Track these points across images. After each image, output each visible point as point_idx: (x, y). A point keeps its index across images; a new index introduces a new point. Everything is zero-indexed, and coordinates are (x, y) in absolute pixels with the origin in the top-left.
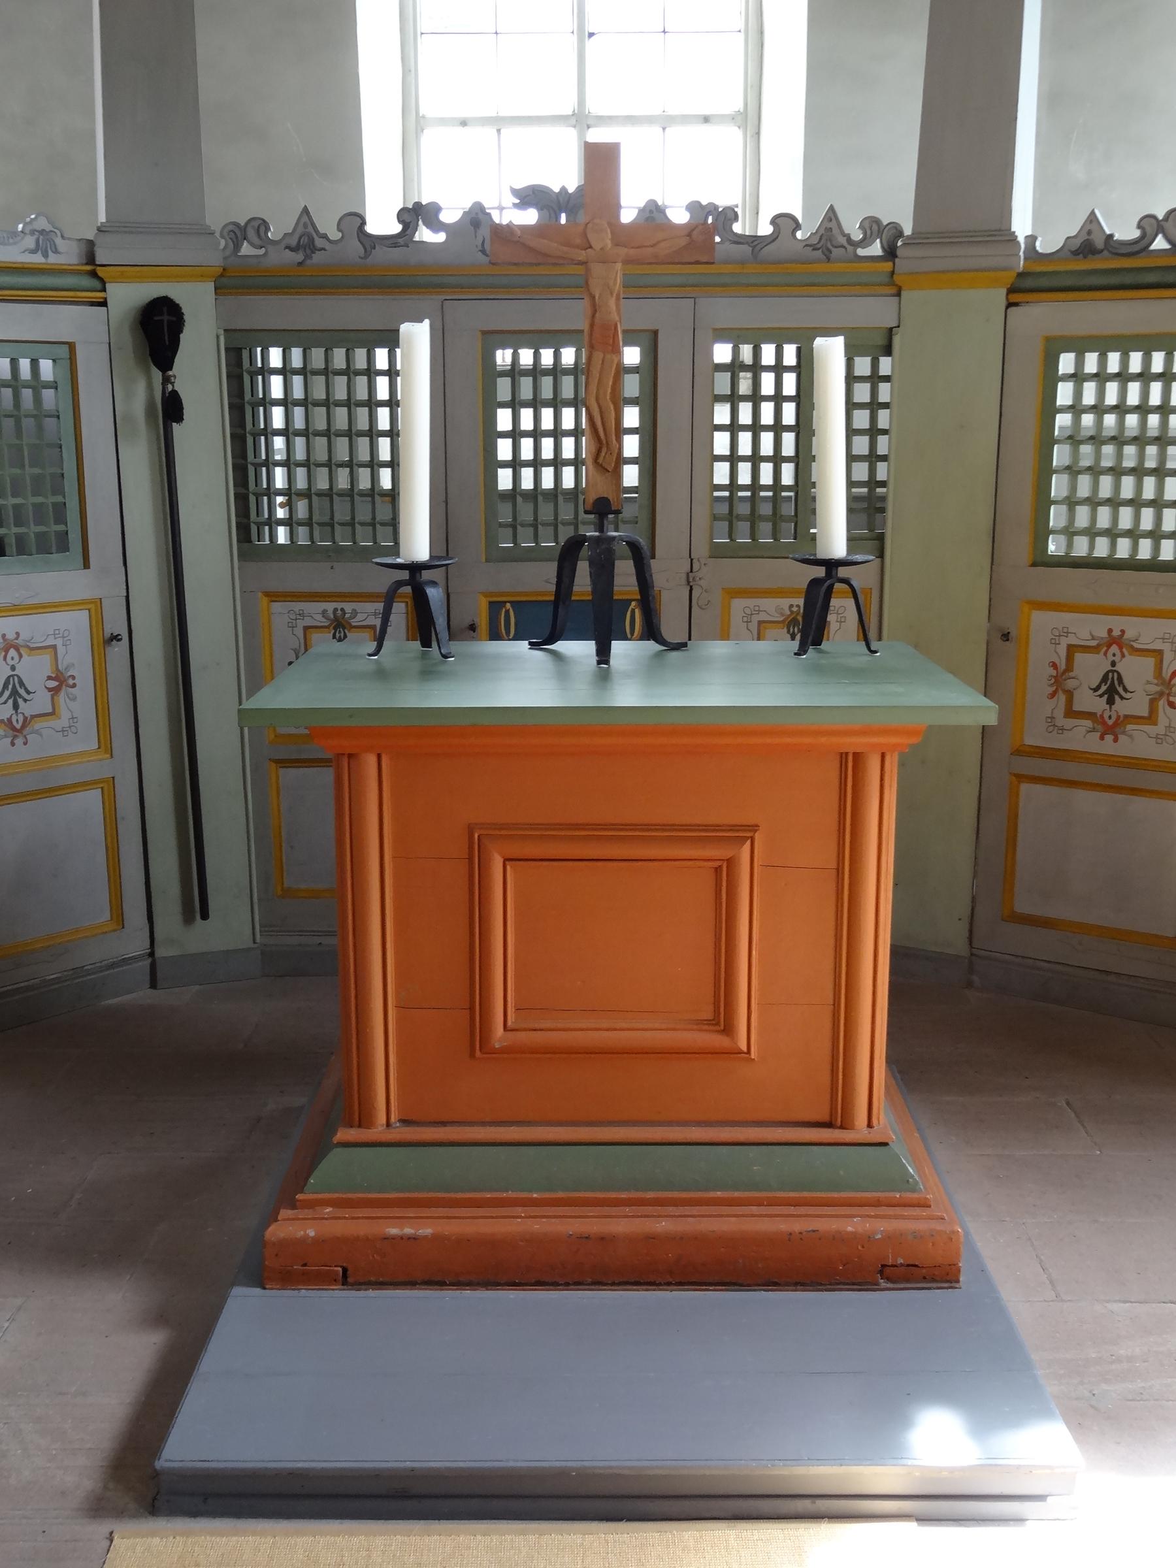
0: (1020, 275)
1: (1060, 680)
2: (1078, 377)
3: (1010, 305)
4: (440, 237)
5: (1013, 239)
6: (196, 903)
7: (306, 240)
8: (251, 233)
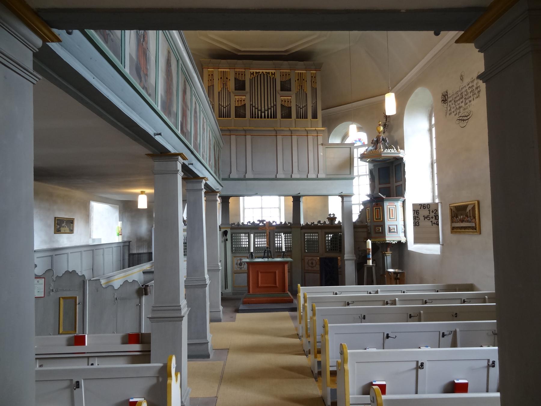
1: (308, 263)
6: (226, 287)
7: (238, 224)
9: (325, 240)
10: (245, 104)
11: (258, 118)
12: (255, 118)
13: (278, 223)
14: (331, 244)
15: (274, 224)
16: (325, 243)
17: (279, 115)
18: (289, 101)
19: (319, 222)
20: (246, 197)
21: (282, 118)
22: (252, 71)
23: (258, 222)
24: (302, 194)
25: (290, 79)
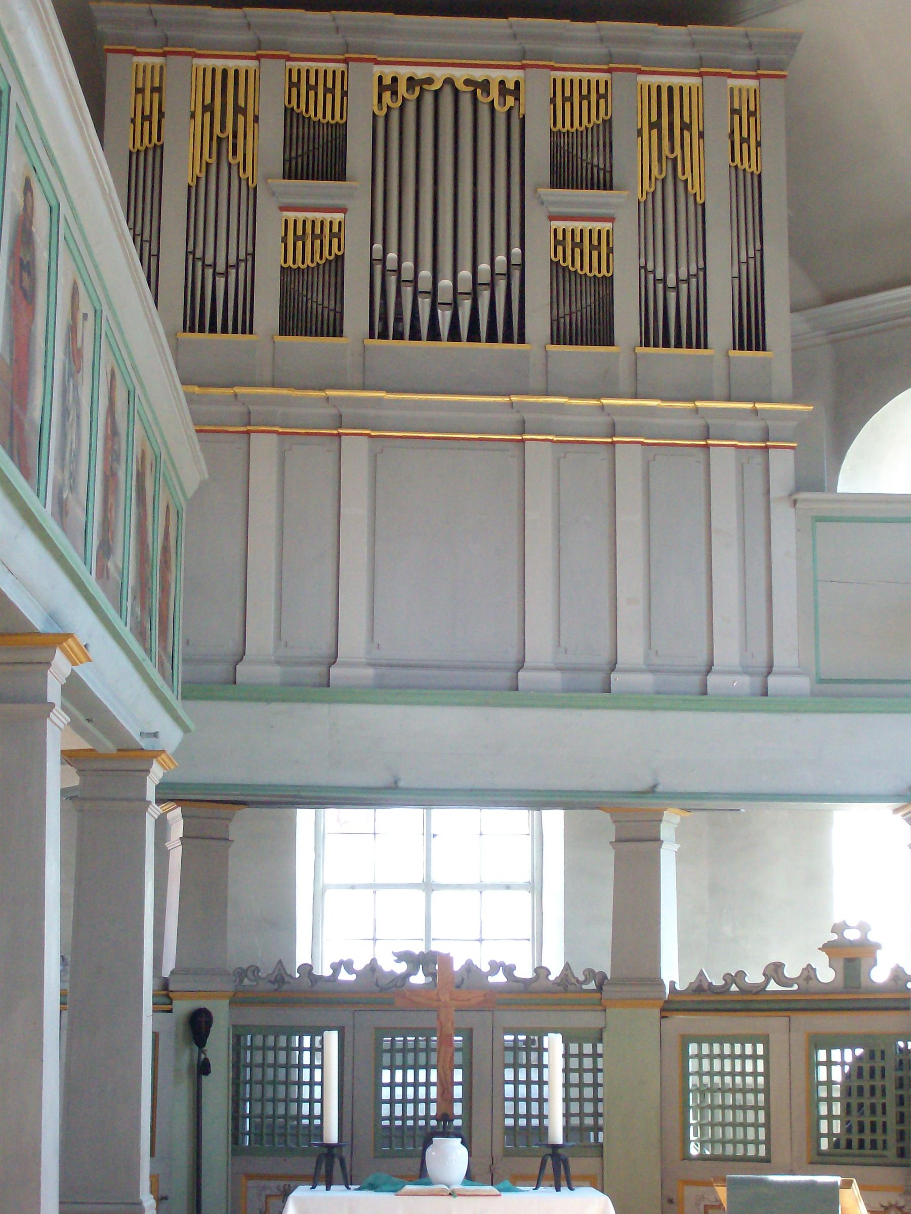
0: (666, 1002)
2: (700, 1057)
3: (662, 1017)
4: (353, 977)
5: (661, 984)
7: (280, 977)
8: (250, 974)
9: (812, 1084)
10: (340, 259)
11: (415, 335)
12: (398, 336)
13: (524, 972)
14: (847, 1109)
15: (500, 978)
16: (813, 1102)
17: (538, 322)
18: (601, 246)
19: (775, 970)
20: (331, 814)
21: (557, 338)
22: (388, 72)
23: (401, 968)
24: (667, 783)
25: (608, 124)
